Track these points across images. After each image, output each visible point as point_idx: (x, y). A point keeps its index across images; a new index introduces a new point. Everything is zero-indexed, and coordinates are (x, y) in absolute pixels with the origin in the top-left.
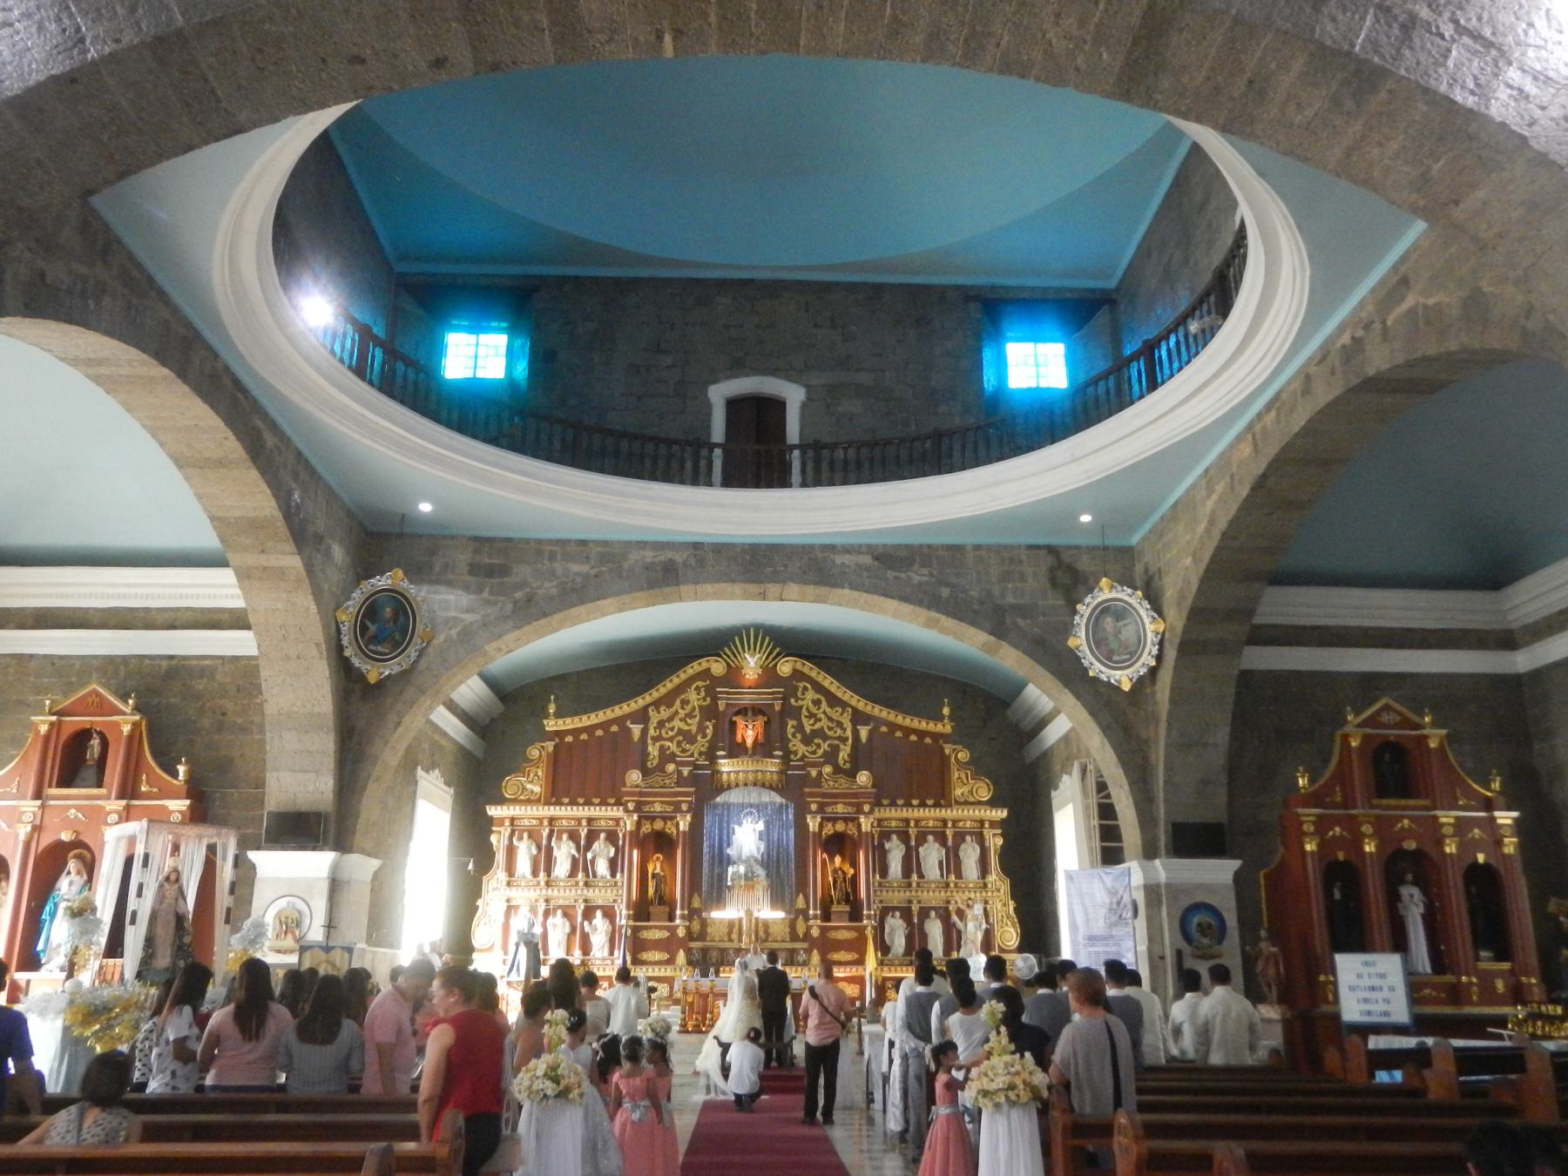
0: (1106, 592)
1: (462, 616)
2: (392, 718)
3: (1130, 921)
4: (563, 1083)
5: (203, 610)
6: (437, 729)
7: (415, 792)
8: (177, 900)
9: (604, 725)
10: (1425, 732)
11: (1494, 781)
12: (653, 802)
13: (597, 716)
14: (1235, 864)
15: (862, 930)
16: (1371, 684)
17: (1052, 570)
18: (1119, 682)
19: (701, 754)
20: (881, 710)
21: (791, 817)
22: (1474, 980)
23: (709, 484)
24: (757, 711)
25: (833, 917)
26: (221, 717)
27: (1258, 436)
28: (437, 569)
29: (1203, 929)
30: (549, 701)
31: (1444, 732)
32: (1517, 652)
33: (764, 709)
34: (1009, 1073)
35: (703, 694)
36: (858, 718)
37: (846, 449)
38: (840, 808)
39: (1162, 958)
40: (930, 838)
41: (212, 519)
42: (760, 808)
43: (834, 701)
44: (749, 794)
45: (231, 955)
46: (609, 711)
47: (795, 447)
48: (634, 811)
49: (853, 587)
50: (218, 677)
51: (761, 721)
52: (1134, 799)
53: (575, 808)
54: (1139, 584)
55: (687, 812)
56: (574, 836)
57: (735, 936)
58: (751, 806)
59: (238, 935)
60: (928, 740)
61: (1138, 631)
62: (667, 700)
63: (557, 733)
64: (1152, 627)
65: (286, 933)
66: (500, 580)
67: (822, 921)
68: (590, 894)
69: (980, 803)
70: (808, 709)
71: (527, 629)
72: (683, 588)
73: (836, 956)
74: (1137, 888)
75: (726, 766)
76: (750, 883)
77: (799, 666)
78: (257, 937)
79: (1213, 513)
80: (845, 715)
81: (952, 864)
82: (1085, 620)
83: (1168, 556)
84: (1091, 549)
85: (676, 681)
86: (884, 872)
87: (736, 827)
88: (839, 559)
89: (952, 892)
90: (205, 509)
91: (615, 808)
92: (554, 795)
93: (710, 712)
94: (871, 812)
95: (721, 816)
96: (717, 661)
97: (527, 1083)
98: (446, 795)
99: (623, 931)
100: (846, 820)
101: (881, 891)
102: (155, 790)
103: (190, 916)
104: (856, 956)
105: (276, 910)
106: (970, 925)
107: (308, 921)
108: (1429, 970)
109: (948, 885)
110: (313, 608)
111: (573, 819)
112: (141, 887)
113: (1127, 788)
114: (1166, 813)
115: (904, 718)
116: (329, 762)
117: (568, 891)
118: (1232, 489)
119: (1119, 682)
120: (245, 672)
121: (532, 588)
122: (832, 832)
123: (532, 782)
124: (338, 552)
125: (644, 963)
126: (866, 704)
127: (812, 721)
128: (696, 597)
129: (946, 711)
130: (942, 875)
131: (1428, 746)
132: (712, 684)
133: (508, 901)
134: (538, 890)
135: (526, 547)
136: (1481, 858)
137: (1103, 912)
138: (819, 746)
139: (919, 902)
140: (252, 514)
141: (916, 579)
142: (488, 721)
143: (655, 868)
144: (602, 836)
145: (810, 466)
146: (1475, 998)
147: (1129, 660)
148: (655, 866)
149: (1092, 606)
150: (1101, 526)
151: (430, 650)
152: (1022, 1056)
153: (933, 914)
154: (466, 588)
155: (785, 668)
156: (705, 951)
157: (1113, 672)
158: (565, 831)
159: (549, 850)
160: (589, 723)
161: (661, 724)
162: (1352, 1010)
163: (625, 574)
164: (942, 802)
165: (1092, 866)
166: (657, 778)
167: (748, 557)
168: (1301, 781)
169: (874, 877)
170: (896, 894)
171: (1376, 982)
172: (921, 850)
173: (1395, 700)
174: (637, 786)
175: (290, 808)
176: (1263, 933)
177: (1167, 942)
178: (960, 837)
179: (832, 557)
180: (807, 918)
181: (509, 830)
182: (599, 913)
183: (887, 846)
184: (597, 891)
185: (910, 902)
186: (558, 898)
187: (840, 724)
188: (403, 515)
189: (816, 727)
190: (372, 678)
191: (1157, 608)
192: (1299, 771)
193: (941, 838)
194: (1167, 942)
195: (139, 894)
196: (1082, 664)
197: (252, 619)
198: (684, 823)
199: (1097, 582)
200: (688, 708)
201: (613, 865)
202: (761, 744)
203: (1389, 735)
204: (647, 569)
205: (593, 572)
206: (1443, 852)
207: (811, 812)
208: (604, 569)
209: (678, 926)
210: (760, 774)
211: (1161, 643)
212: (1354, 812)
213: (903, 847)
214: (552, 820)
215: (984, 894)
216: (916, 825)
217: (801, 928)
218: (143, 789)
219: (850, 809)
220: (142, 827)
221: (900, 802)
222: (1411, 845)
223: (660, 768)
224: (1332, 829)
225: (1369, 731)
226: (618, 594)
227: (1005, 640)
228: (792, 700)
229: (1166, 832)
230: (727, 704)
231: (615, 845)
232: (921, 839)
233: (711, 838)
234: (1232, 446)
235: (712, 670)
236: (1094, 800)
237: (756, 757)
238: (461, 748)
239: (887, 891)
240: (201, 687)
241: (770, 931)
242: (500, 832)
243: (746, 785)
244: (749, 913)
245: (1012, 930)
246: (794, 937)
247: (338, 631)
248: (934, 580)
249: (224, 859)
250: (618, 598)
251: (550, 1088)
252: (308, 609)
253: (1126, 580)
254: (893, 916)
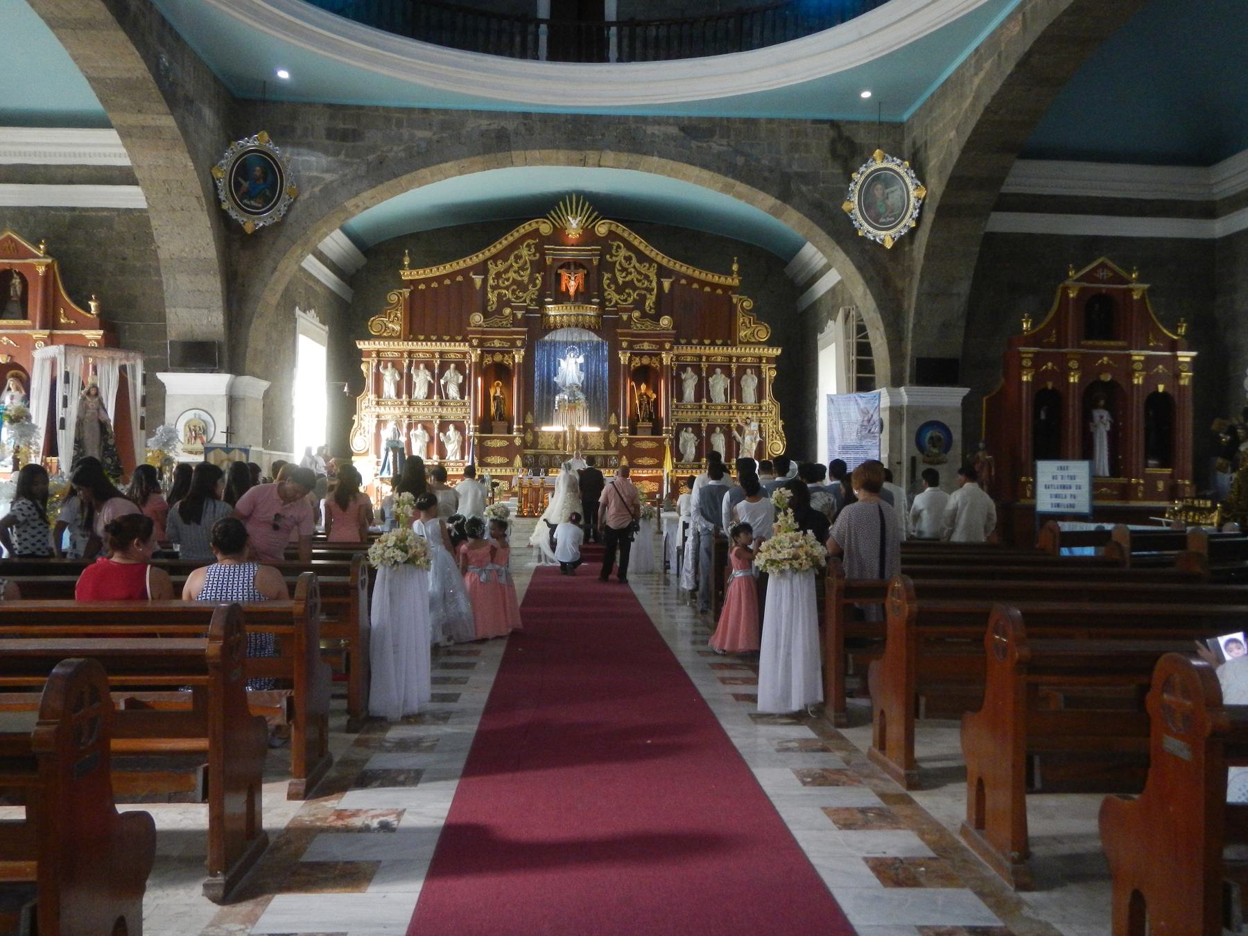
0: (879, 162)
1: (321, 175)
2: (269, 263)
3: (877, 435)
4: (411, 552)
5: (95, 168)
6: (310, 276)
7: (295, 328)
8: (98, 410)
9: (451, 276)
10: (1131, 286)
11: (1181, 327)
12: (494, 339)
13: (445, 267)
14: (965, 391)
15: (661, 441)
16: (1092, 245)
17: (833, 142)
18: (883, 240)
19: (532, 300)
20: (681, 266)
21: (606, 353)
22: (1142, 482)
23: (536, 57)
24: (577, 265)
25: (639, 430)
26: (123, 262)
27: (1028, 16)
28: (299, 132)
29: (934, 441)
30: (404, 255)
31: (1146, 286)
32: (1215, 221)
33: (585, 265)
34: (793, 546)
35: (533, 250)
36: (663, 272)
37: (658, 27)
38: (646, 346)
39: (899, 463)
40: (718, 370)
41: (91, 79)
42: (581, 345)
43: (642, 258)
44: (572, 334)
45: (149, 454)
46: (454, 264)
47: (612, 24)
48: (478, 346)
49: (661, 156)
50: (116, 226)
51: (581, 274)
52: (888, 338)
53: (429, 343)
54: (906, 156)
55: (522, 347)
56: (429, 366)
57: (560, 445)
58: (573, 343)
59: (153, 439)
60: (719, 291)
61: (902, 197)
62: (502, 256)
63: (411, 282)
64: (915, 193)
65: (195, 438)
66: (352, 144)
67: (630, 435)
68: (444, 411)
69: (760, 343)
70: (620, 264)
71: (380, 187)
72: (515, 153)
73: (640, 461)
74: (885, 409)
75: (553, 310)
77: (613, 228)
78: (171, 438)
79: (979, 86)
80: (652, 269)
81: (735, 391)
82: (858, 187)
83: (934, 131)
84: (869, 125)
85: (511, 239)
86: (680, 395)
87: (562, 361)
88: (650, 129)
89: (734, 412)
90: (82, 70)
91: (462, 344)
92: (411, 333)
93: (539, 266)
94: (671, 349)
95: (549, 355)
96: (545, 222)
97: (379, 552)
98: (323, 331)
99: (472, 440)
100: (650, 355)
101: (678, 412)
102: (72, 322)
103: (112, 424)
104: (656, 461)
105: (185, 421)
106: (748, 438)
107: (213, 429)
108: (1107, 474)
109: (730, 408)
110: (190, 164)
111: (427, 352)
112: (65, 399)
113: (882, 329)
114: (912, 350)
115: (700, 273)
116: (218, 301)
117: (426, 409)
118: (999, 65)
119: (883, 240)
120: (137, 220)
121: (383, 151)
122: (639, 365)
123: (392, 322)
124: (208, 114)
125: (488, 465)
126: (669, 261)
128: (526, 163)
129: (735, 267)
130: (726, 400)
131: (1132, 297)
132: (541, 242)
133: (378, 416)
134: (402, 409)
135: (376, 113)
136: (1161, 388)
137: (856, 427)
138: (629, 295)
139: (707, 420)
140: (127, 75)
141: (716, 148)
142: (354, 271)
143: (496, 392)
144: (452, 366)
145: (625, 42)
146: (1140, 495)
147: (891, 222)
148: (495, 391)
149: (866, 174)
150: (877, 102)
151: (297, 205)
152: (805, 533)
153: (718, 429)
154: (326, 151)
155: (602, 229)
156: (536, 456)
157: (879, 232)
158: (422, 362)
159: (410, 377)
160: (438, 274)
161: (498, 275)
162: (1045, 502)
163: (463, 140)
164: (729, 342)
165: (849, 392)
166: (496, 319)
167: (570, 126)
168: (1025, 326)
169: (672, 400)
170: (689, 413)
171: (1067, 482)
172: (710, 380)
173: (1110, 259)
174: (480, 326)
175: (188, 338)
176: (981, 445)
177: (904, 451)
178: (742, 370)
179: (644, 128)
180: (618, 432)
181: (376, 360)
182: (451, 427)
183: (683, 376)
184: (449, 409)
185: (700, 420)
186: (419, 415)
187: (647, 277)
188: (265, 82)
189: (627, 279)
190: (249, 228)
191: (921, 177)
192: (1024, 317)
193: (727, 370)
194: (904, 451)
195: (65, 405)
196: (854, 225)
197: (138, 175)
198: (519, 357)
199: (872, 154)
200: (521, 262)
201: (462, 389)
202: (582, 293)
203: (1101, 288)
204: (482, 136)
205: (435, 138)
206: (1132, 382)
207: (622, 349)
208: (444, 135)
209: (515, 437)
210: (580, 317)
211: (921, 208)
212: (1064, 350)
213: (695, 377)
214: (410, 353)
215: (759, 415)
216: (707, 360)
217: (613, 439)
218: (62, 321)
219: (654, 347)
220: (60, 351)
221: (695, 341)
222: (1106, 377)
223: (499, 311)
224: (1046, 364)
225: (1086, 285)
226: (456, 158)
227: (789, 204)
228: (608, 256)
229: (911, 365)
230: (553, 259)
231: (463, 373)
232: (711, 371)
233: (541, 369)
234: (1003, 25)
235: (541, 231)
236: (854, 340)
237: (579, 304)
238: (332, 292)
239: (682, 412)
240: (103, 235)
241: (589, 441)
242: (368, 362)
243: (569, 326)
244: (572, 427)
245: (780, 442)
246: (607, 446)
247: (215, 186)
248: (731, 149)
249: (134, 377)
250: (459, 161)
251: (399, 555)
252: (186, 166)
253: (895, 152)
254: (686, 431)
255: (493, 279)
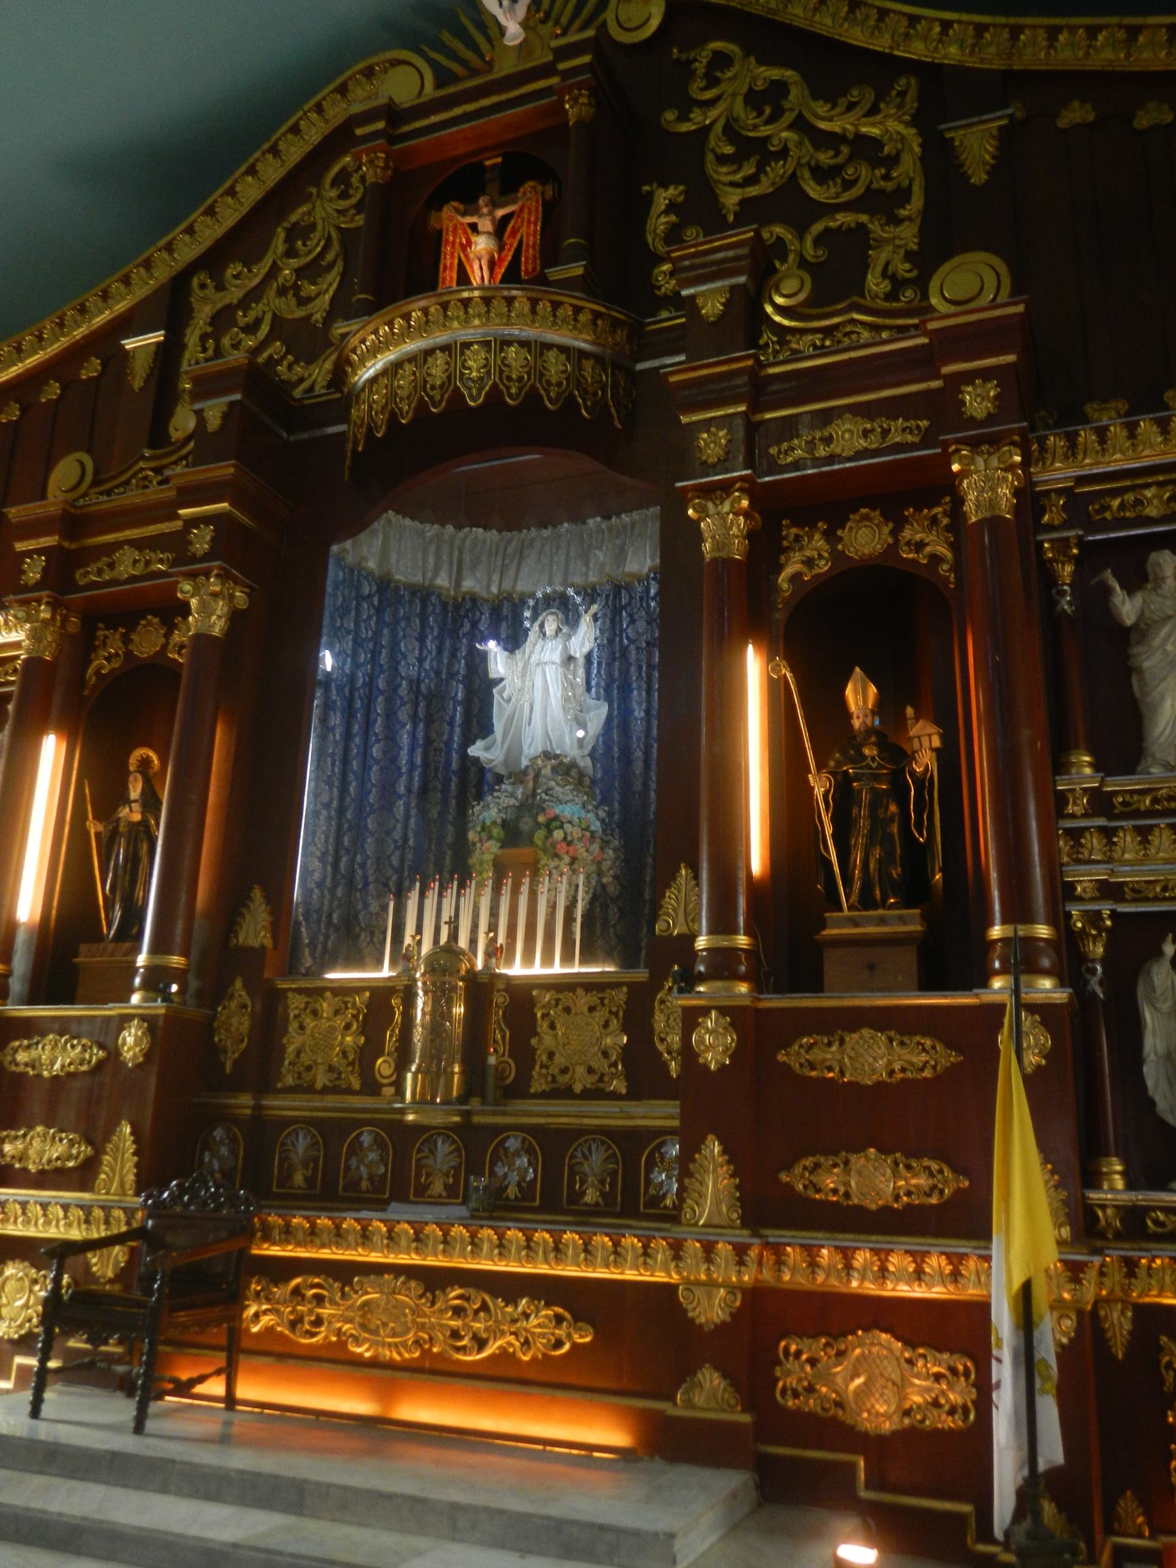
57: (384, 1066)
67: (760, 985)
70: (731, 132)
76: (520, 853)
96: (396, 63)
101: (1108, 834)
104: (952, 1183)
122: (823, 566)
127: (749, 170)
161: (222, 320)
187: (866, 149)
209: (125, 1020)
219: (899, 431)
228: (670, 116)
239: (1144, 833)
241: (545, 1040)
255: (204, 338)
